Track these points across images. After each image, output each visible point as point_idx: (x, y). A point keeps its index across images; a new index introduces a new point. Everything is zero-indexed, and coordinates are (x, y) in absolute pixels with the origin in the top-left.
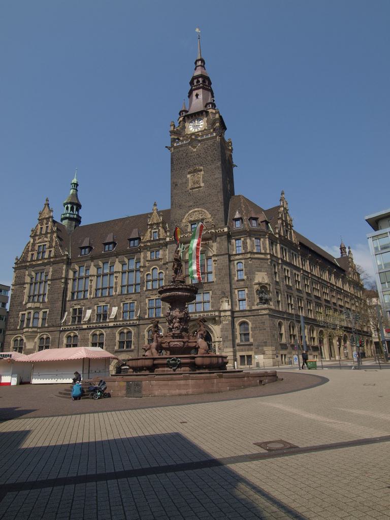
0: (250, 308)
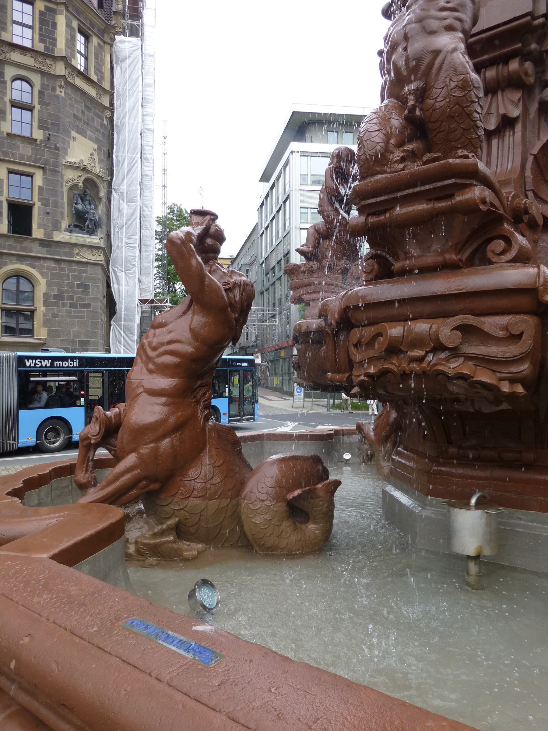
0: (45, 234)
